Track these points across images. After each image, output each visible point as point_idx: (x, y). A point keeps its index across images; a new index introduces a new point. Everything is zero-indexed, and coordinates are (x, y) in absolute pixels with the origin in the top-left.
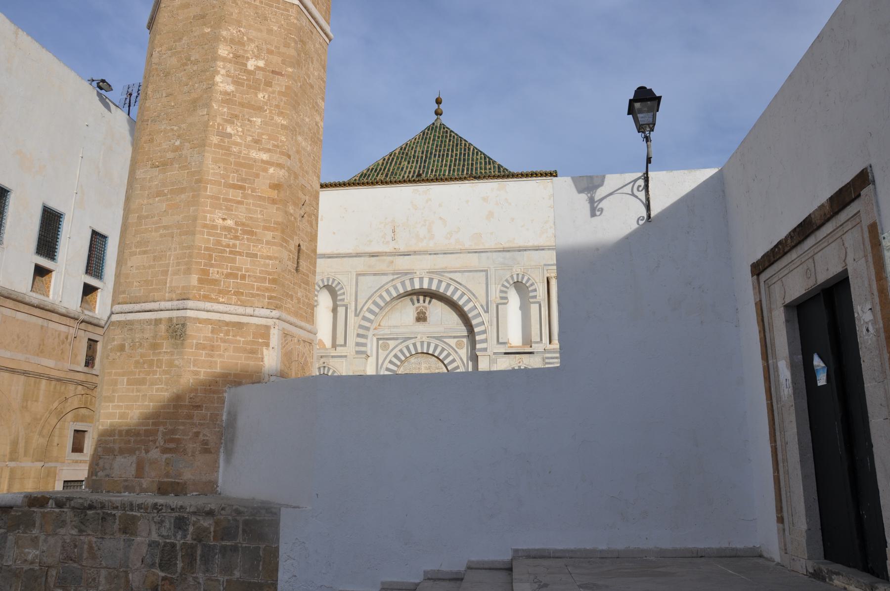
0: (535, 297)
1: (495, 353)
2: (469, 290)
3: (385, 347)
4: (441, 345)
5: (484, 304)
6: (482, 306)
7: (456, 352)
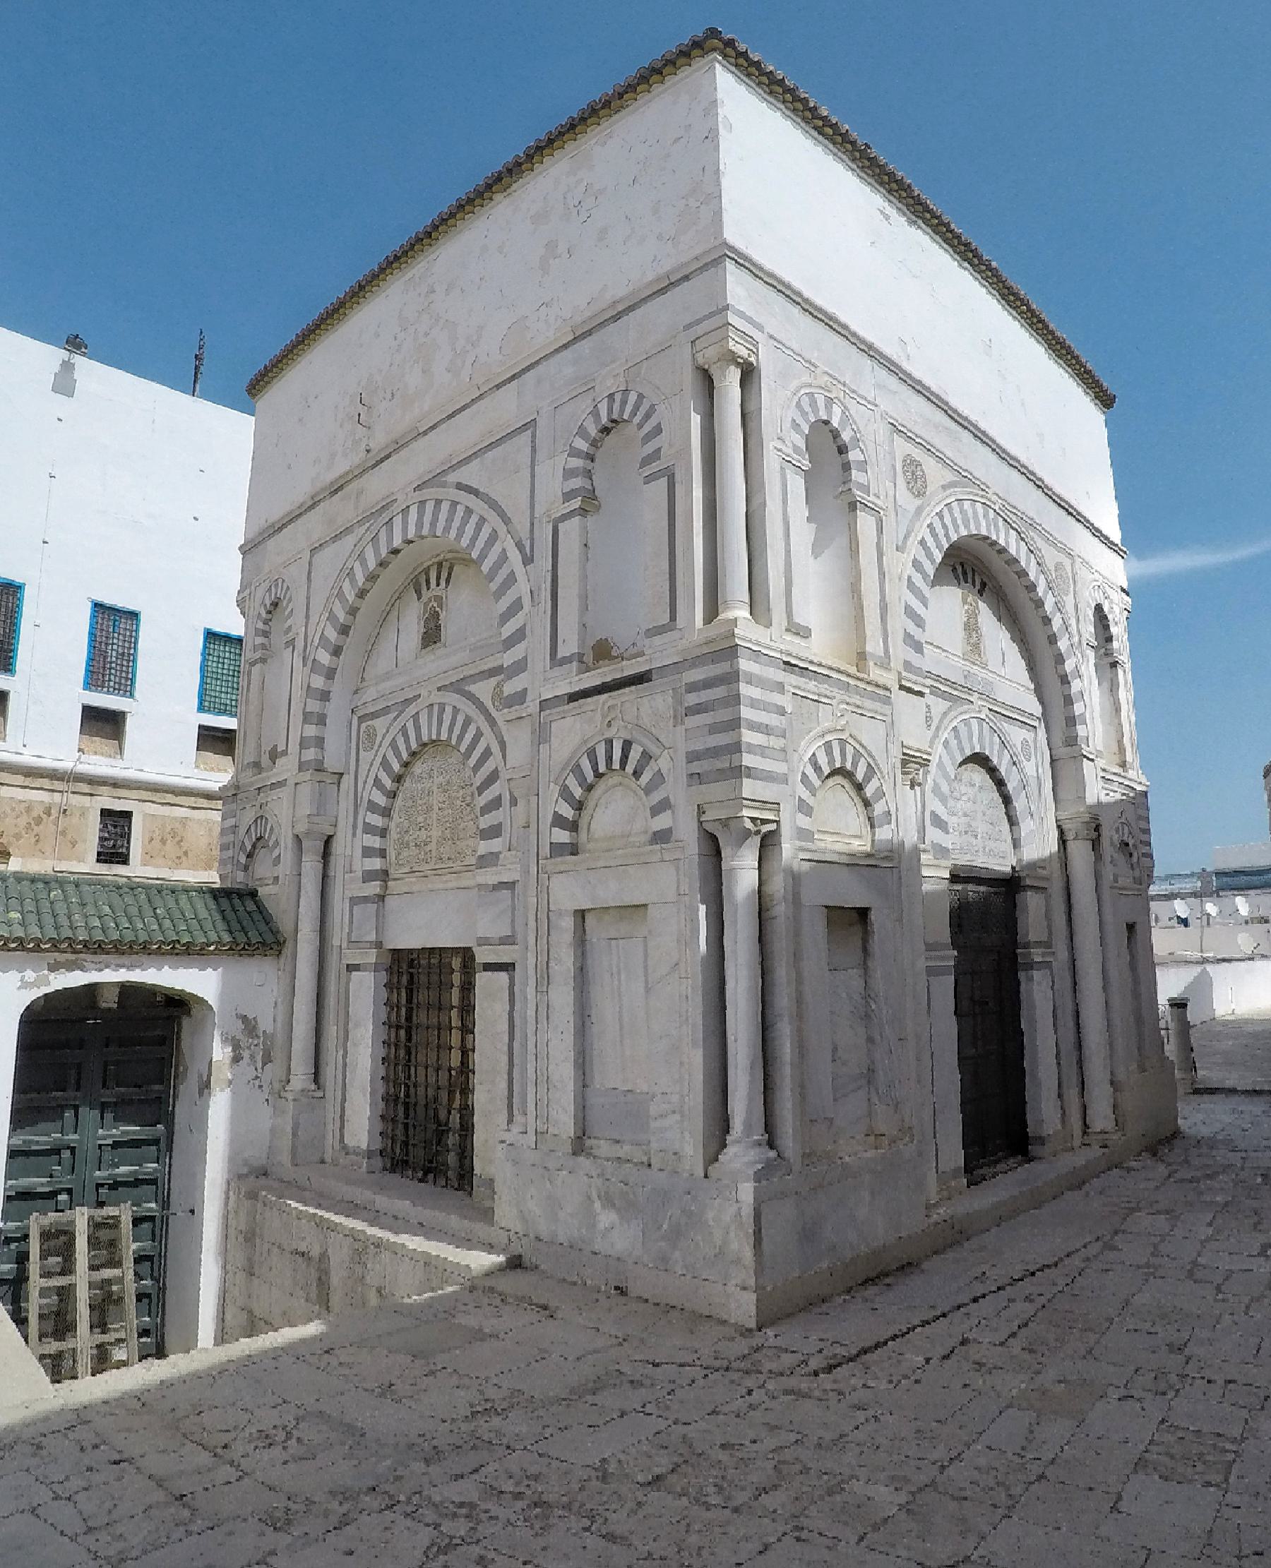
0: (656, 454)
1: (544, 704)
2: (494, 505)
3: (371, 735)
4: (468, 708)
5: (524, 535)
6: (519, 545)
7: (492, 722)
